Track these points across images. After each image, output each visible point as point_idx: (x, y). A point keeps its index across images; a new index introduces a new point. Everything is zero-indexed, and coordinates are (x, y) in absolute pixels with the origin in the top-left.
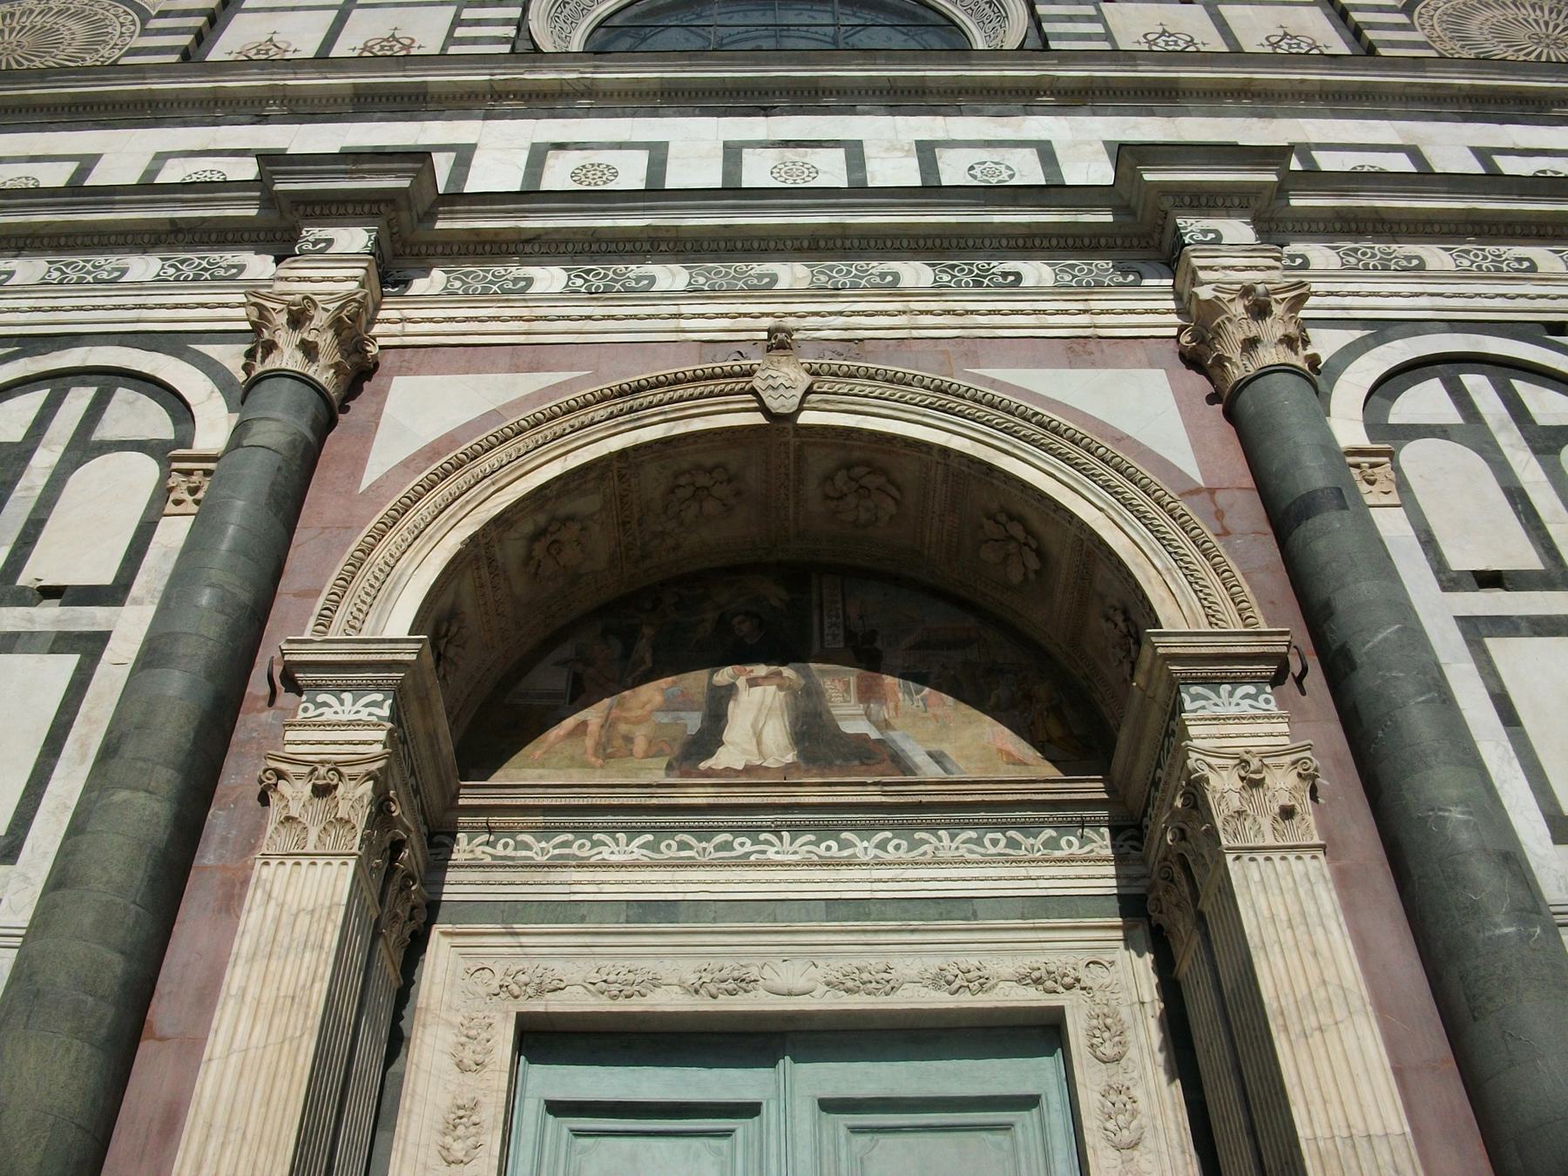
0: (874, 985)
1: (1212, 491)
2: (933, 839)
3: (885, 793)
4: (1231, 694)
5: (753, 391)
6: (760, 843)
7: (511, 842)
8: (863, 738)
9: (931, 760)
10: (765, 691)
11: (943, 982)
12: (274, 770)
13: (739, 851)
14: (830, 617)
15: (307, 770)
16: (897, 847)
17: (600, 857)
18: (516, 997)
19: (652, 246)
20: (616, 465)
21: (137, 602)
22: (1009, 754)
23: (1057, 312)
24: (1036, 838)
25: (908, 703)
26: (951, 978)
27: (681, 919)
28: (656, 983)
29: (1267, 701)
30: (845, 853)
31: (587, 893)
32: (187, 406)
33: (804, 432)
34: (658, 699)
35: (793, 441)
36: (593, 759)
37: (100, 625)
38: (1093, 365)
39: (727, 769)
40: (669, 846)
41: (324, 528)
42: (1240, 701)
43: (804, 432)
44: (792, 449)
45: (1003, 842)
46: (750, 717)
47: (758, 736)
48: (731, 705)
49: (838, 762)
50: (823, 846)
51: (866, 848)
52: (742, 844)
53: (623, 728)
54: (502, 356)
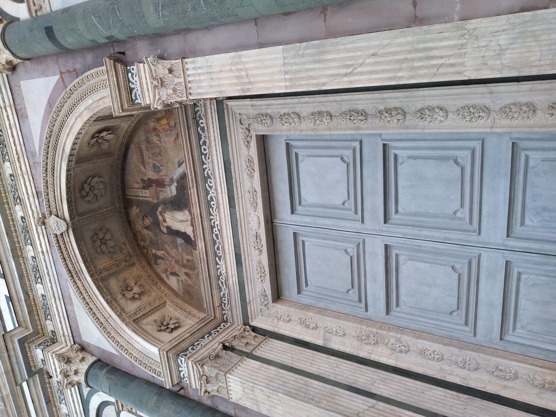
0: (254, 197)
1: (61, 73)
2: (207, 170)
3: (193, 187)
4: (133, 83)
6: (214, 225)
7: (223, 299)
8: (177, 188)
11: (252, 175)
12: (204, 393)
13: (218, 232)
14: (139, 194)
16: (211, 183)
18: (268, 303)
20: (96, 277)
22: (175, 140)
23: (9, 120)
25: (163, 171)
26: (250, 172)
28: (260, 262)
31: (235, 279)
32: (103, 402)
33: (72, 217)
34: (174, 250)
35: (77, 218)
36: (196, 272)
38: (25, 109)
43: (72, 217)
44: (80, 218)
45: (205, 147)
46: (176, 223)
47: (182, 221)
49: (186, 197)
50: (213, 206)
51: (212, 193)
52: (216, 231)
53: (185, 262)
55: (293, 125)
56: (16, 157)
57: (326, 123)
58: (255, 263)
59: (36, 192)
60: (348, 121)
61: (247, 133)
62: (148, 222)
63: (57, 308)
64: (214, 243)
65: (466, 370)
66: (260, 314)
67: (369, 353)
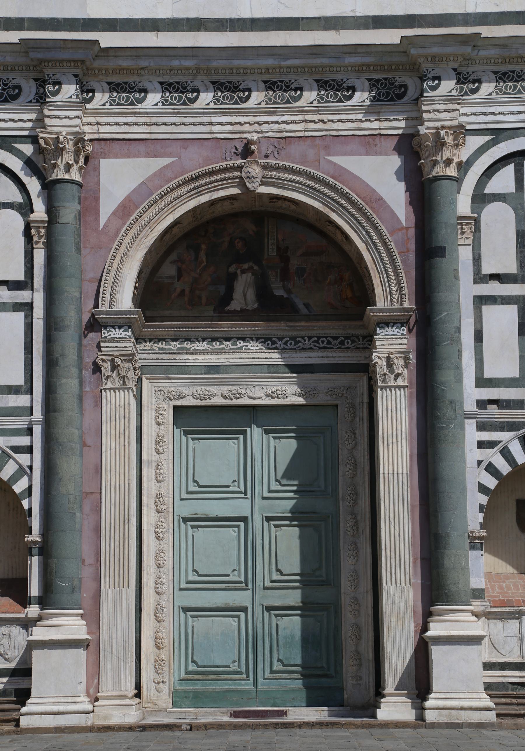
1: (407, 229)
2: (303, 341)
5: (241, 177)
9: (303, 306)
10: (247, 275)
12: (101, 359)
15: (110, 358)
17: (193, 348)
19: (197, 72)
21: (38, 291)
24: (337, 340)
27: (222, 371)
28: (214, 395)
29: (403, 330)
30: (274, 346)
31: (190, 362)
36: (188, 306)
37: (26, 299)
38: (376, 153)
39: (235, 310)
40: (216, 344)
41: (92, 248)
42: (395, 330)
45: (325, 343)
47: (245, 296)
48: (235, 283)
50: (266, 343)
51: (280, 344)
54: (141, 147)
55: (346, 442)
56: (325, 118)
57: (347, 473)
58: (212, 389)
59: (285, 138)
60: (349, 492)
61: (340, 395)
62: (239, 245)
63: (136, 124)
64: (228, 339)
65: (154, 586)
66: (157, 389)
67: (148, 504)
